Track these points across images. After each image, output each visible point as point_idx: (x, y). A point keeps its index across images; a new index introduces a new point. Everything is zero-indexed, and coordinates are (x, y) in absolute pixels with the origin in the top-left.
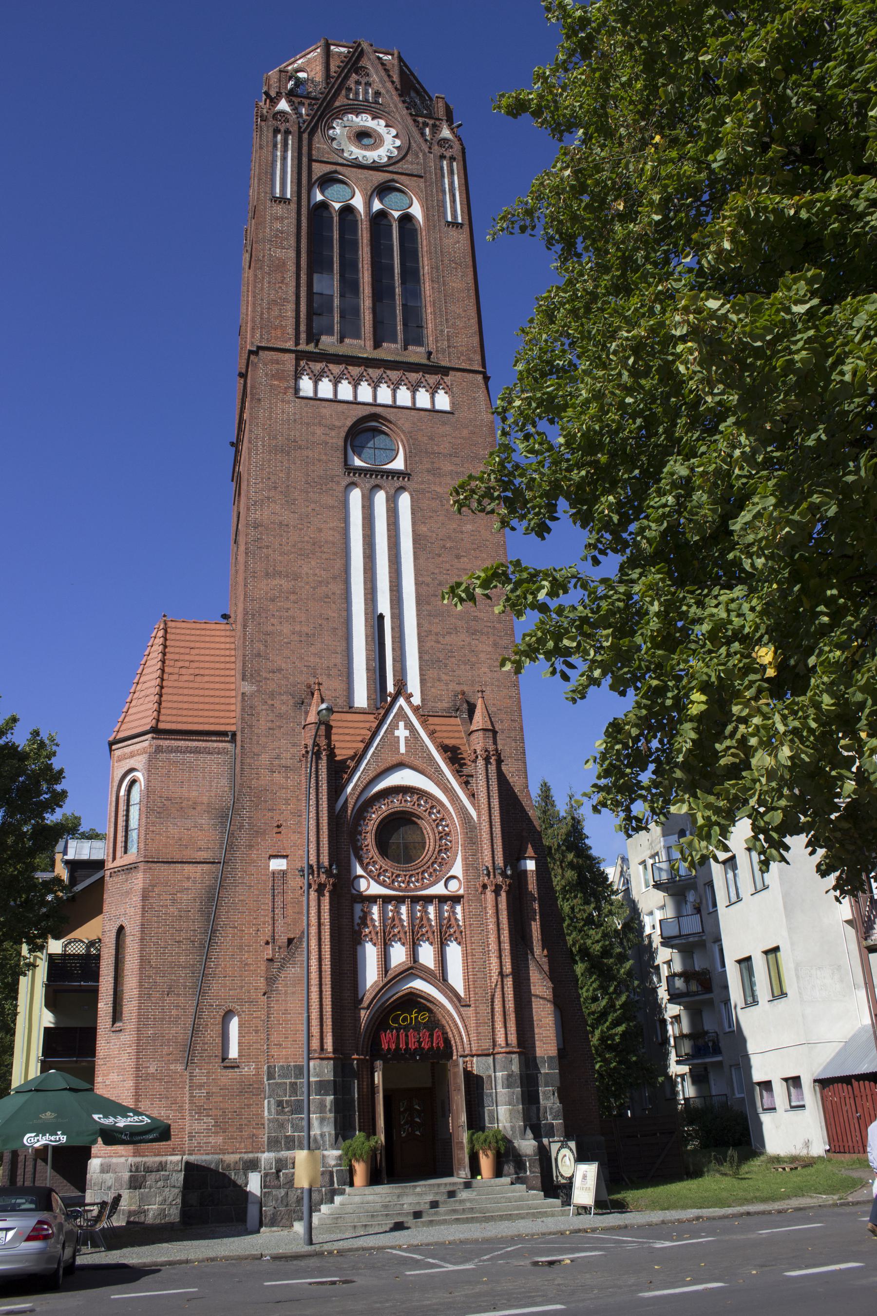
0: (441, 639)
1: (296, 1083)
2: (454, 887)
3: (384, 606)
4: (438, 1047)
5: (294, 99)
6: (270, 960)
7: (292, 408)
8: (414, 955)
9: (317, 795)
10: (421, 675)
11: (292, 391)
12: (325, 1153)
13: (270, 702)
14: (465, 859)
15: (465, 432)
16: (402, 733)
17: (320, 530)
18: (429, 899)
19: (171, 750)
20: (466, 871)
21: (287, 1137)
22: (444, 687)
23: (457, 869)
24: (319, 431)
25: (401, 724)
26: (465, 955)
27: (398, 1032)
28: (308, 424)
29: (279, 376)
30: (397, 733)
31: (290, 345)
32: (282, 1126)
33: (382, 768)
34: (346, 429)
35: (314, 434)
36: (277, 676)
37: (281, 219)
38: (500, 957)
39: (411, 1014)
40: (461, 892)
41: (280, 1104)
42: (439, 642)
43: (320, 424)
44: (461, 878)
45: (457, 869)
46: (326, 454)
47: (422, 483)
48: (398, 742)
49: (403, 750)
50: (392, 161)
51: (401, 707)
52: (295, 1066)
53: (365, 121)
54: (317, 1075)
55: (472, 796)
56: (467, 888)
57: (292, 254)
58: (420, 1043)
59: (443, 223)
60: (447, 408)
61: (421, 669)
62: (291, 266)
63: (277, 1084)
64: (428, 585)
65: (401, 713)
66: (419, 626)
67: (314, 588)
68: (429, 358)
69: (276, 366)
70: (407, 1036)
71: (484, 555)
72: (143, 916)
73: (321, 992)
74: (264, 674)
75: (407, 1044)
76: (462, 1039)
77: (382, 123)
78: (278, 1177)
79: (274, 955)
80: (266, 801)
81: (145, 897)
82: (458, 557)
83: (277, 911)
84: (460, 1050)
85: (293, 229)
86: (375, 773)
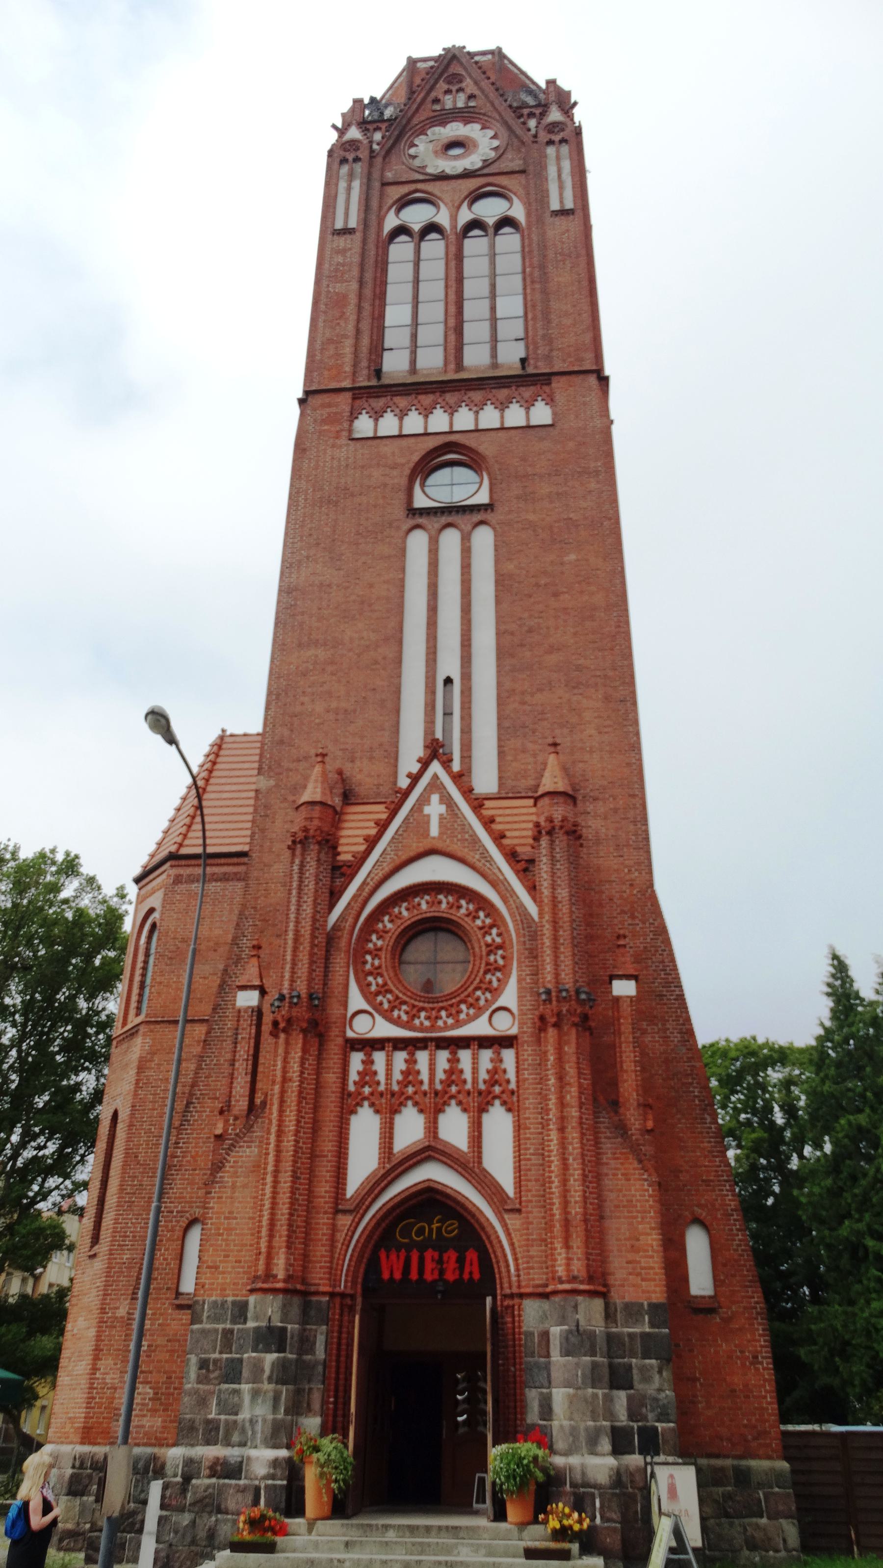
0: (528, 698)
1: (231, 1331)
2: (504, 1025)
3: (449, 664)
4: (471, 1279)
5: (368, 126)
6: (218, 1137)
7: (345, 452)
8: (432, 1128)
9: (299, 897)
10: (500, 747)
11: (345, 434)
12: (253, 1453)
13: (291, 798)
14: (520, 980)
15: (571, 445)
16: (435, 809)
17: (371, 586)
18: (465, 1042)
19: (192, 879)
20: (520, 998)
21: (208, 1422)
22: (531, 760)
23: (509, 997)
24: (376, 473)
25: (435, 798)
26: (518, 1128)
27: (408, 1251)
28: (363, 467)
29: (331, 420)
30: (427, 810)
31: (347, 384)
32: (202, 1402)
33: (404, 857)
34: (412, 465)
35: (370, 476)
36: (303, 765)
37: (343, 252)
38: (562, 1130)
39: (430, 1224)
40: (514, 1031)
41: (204, 1364)
42: (523, 703)
43: (378, 465)
44: (515, 1010)
45: (509, 997)
46: (384, 497)
47: (510, 512)
48: (428, 823)
49: (434, 831)
50: (487, 164)
51: (435, 777)
52: (234, 1303)
53: (455, 130)
54: (256, 1318)
55: (532, 889)
56: (521, 1025)
57: (354, 286)
58: (442, 1272)
59: (548, 214)
60: (549, 422)
61: (500, 739)
62: (353, 299)
63: (203, 1331)
64: (512, 634)
65: (435, 785)
66: (499, 684)
67: (359, 655)
68: (523, 368)
69: (328, 410)
70: (422, 1260)
71: (593, 588)
72: (136, 1094)
73: (276, 1182)
74: (285, 764)
75: (421, 1271)
76: (508, 1266)
77: (477, 126)
78: (184, 1490)
79: (225, 1130)
80: (275, 925)
81: (141, 1069)
82: (556, 595)
83: (237, 1064)
84: (506, 1285)
85: (356, 259)
86: (391, 866)
